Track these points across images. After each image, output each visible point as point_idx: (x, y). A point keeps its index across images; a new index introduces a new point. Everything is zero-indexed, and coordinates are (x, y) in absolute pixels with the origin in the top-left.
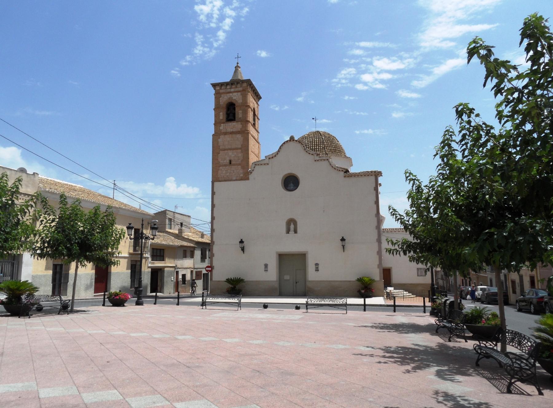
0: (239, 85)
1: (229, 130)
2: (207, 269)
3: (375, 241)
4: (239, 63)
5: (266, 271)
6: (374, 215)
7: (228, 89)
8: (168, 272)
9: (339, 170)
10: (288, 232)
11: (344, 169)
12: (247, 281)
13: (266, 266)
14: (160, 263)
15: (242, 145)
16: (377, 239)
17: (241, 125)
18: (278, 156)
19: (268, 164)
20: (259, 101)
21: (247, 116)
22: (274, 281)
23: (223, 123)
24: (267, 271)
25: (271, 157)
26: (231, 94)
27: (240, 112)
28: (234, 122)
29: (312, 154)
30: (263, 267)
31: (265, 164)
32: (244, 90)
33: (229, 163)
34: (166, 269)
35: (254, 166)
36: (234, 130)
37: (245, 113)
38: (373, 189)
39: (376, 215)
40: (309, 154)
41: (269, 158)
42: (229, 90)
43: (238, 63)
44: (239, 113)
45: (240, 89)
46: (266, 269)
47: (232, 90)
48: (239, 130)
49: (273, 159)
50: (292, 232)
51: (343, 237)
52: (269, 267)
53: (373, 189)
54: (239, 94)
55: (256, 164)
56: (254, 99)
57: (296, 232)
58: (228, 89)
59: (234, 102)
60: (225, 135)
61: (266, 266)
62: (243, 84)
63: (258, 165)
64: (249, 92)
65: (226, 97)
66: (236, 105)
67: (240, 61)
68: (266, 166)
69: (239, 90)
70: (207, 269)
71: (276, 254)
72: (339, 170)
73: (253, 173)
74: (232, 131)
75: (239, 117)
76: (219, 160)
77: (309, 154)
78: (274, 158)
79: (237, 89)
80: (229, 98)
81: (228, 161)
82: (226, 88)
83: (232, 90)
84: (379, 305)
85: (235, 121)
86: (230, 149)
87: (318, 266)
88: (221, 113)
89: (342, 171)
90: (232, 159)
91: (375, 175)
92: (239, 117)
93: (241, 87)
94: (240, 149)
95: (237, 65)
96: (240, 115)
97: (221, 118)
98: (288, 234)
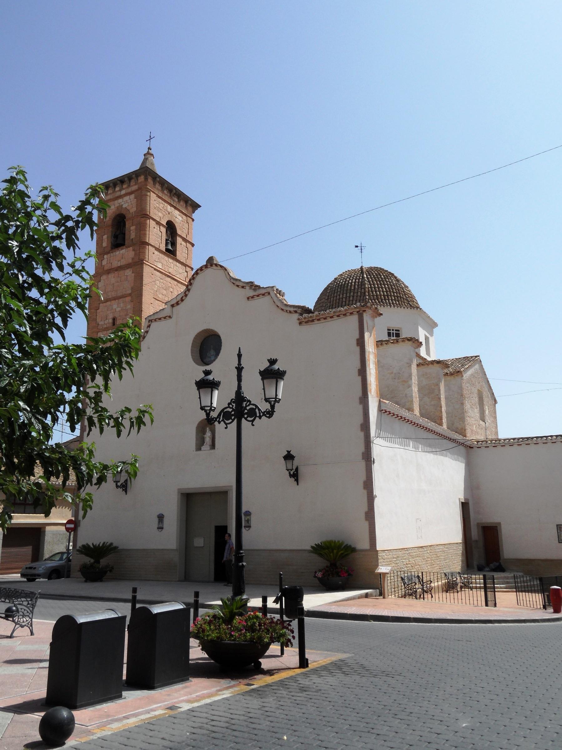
0: (133, 182)
1: (116, 264)
2: (68, 526)
3: (360, 457)
4: (151, 147)
5: (160, 528)
6: (357, 400)
7: (117, 191)
8: (55, 534)
9: (290, 312)
10: (199, 448)
11: (299, 307)
12: (123, 550)
13: (161, 518)
14: (27, 517)
15: (132, 288)
16: (363, 453)
17: (133, 253)
18: (187, 300)
19: (170, 317)
20: (194, 212)
21: (145, 234)
22: (172, 550)
23: (107, 253)
24: (162, 528)
25: (174, 302)
26: (120, 201)
27: (133, 228)
28: (122, 249)
29: (243, 287)
30: (156, 520)
31: (165, 318)
32: (140, 189)
33: (111, 325)
34: (48, 528)
35: (147, 324)
36: (123, 262)
37: (142, 228)
38: (355, 342)
39: (360, 398)
40: (238, 286)
41: (173, 306)
42: (118, 194)
43: (149, 149)
44: (131, 231)
45: (134, 188)
46: (161, 526)
47: (123, 192)
48: (130, 261)
49: (179, 306)
50: (206, 447)
51: (289, 452)
52: (166, 520)
53: (355, 342)
54: (132, 196)
55: (151, 320)
56: (172, 205)
57: (213, 446)
58: (117, 191)
59: (124, 212)
60: (108, 273)
61: (161, 518)
62: (139, 178)
63: (155, 320)
64: (149, 191)
65: (113, 207)
66: (128, 216)
67: (154, 144)
68: (169, 321)
69: (133, 190)
70: (68, 526)
71: (178, 492)
72: (290, 312)
73: (148, 336)
74: (119, 265)
75: (131, 238)
76: (98, 320)
77: (238, 286)
78: (182, 305)
79: (129, 190)
80: (118, 208)
81: (111, 321)
82: (114, 191)
83: (123, 192)
84: (101, 598)
85: (124, 247)
86: (115, 299)
87: (249, 517)
88: (105, 237)
89: (296, 312)
90: (117, 316)
91: (358, 312)
92: (131, 238)
93: (135, 185)
94: (130, 295)
95: (148, 151)
96: (133, 235)
97: (105, 244)
98: (199, 452)
